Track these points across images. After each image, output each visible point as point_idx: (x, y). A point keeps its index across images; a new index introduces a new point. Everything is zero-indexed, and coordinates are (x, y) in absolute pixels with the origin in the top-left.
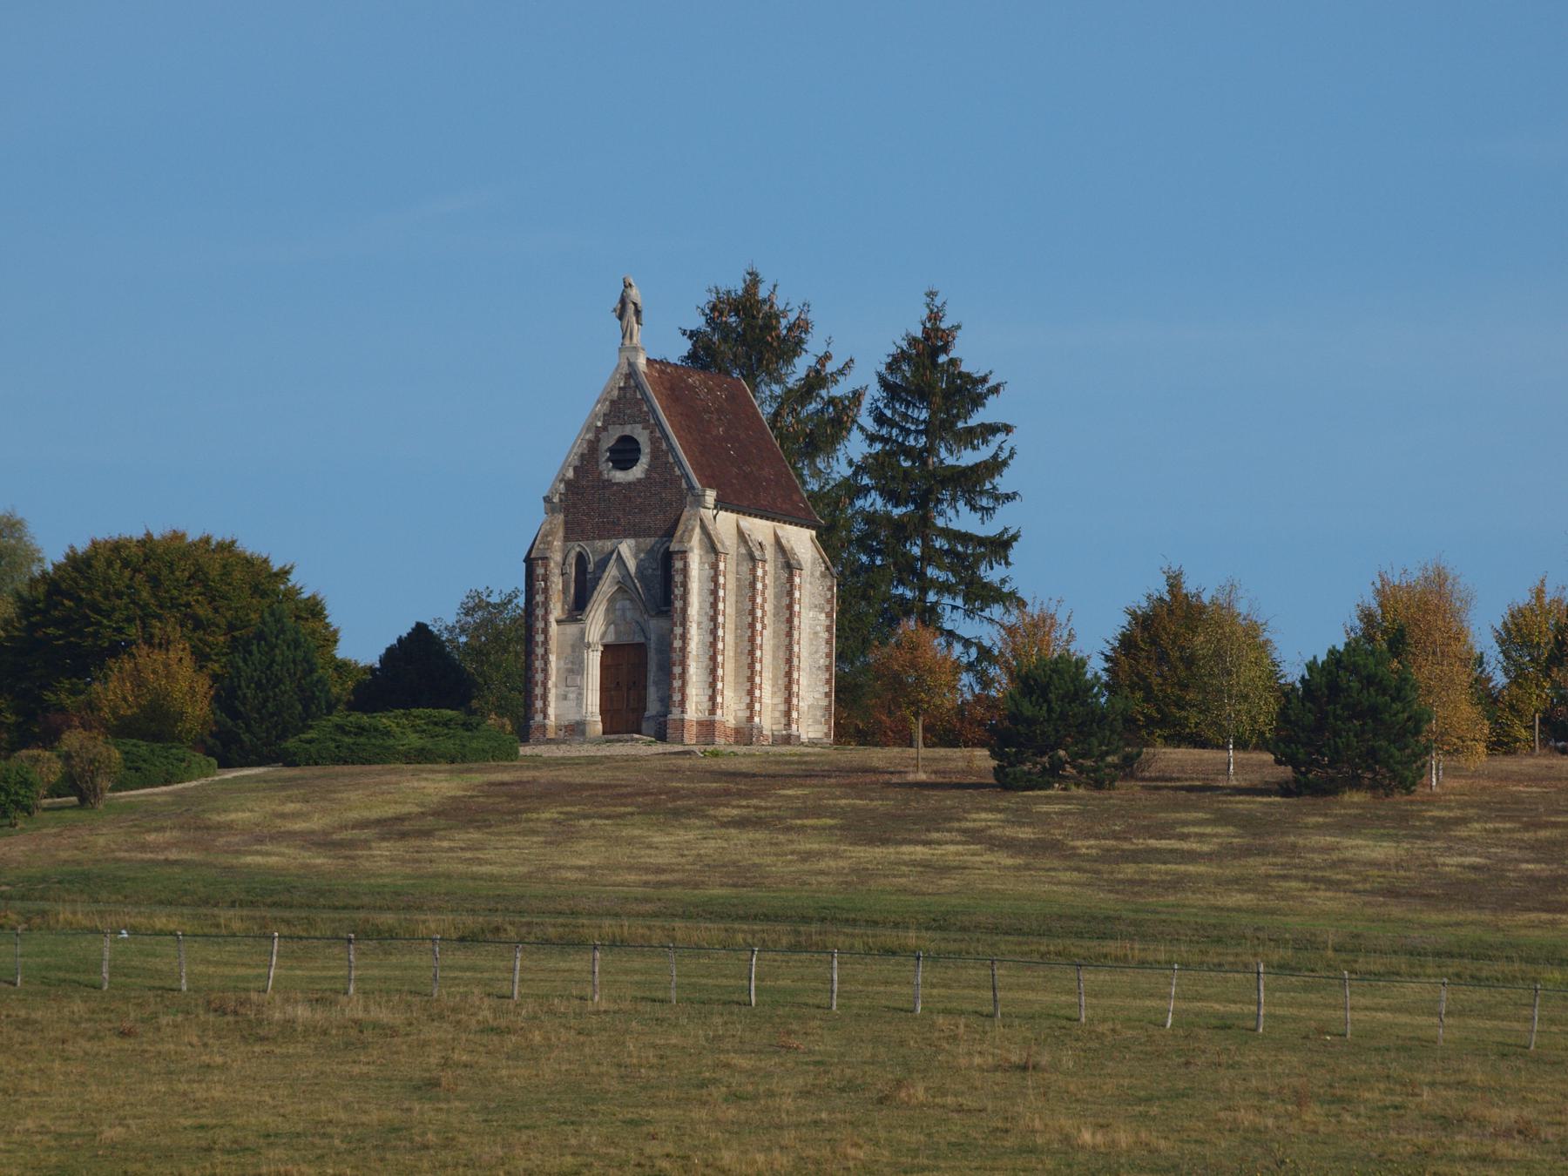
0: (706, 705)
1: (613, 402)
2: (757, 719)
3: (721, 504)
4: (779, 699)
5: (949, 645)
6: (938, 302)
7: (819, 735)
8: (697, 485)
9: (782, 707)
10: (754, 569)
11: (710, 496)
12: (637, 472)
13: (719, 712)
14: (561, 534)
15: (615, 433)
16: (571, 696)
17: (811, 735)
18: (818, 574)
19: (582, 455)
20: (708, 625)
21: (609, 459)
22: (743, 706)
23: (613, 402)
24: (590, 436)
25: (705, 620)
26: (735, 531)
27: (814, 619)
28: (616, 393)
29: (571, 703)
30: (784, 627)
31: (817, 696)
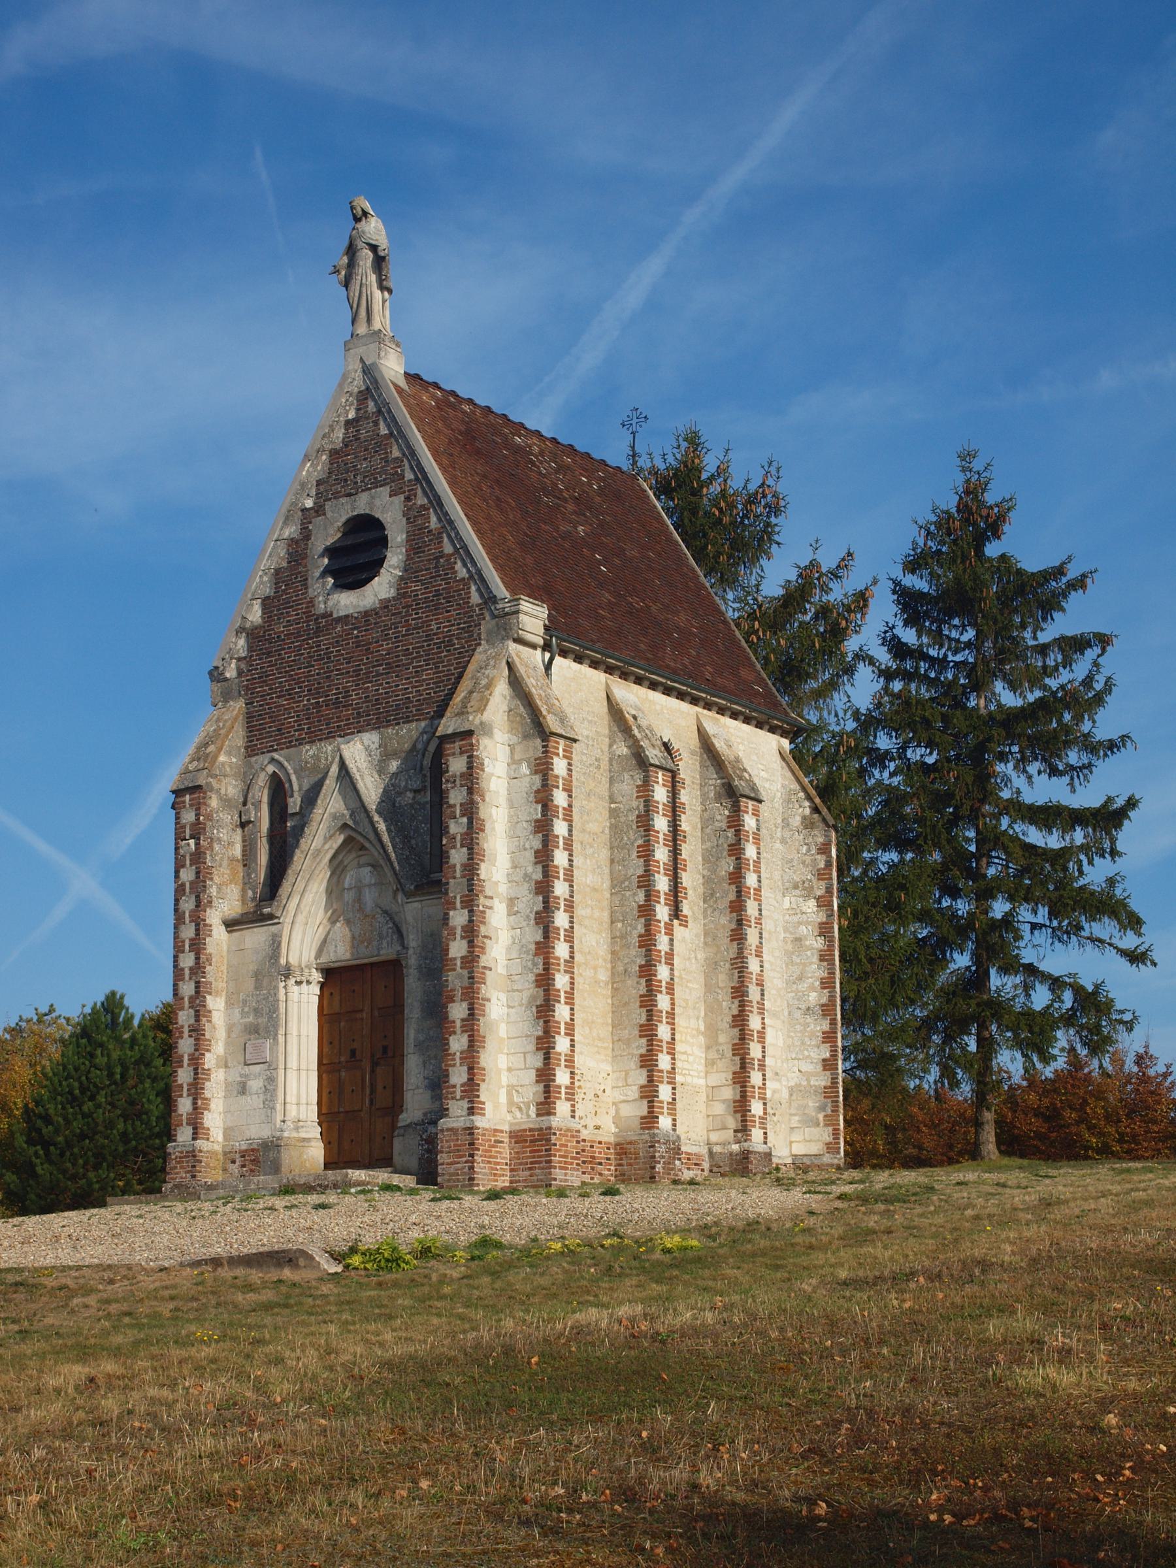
0: (531, 1092)
1: (334, 454)
2: (664, 1122)
3: (564, 639)
4: (722, 1076)
5: (1027, 988)
6: (977, 465)
7: (814, 1149)
9: (729, 1093)
10: (645, 788)
11: (533, 617)
12: (381, 588)
13: (562, 1107)
14: (238, 737)
15: (340, 513)
16: (255, 1085)
17: (799, 1149)
18: (796, 821)
19: (278, 571)
20: (530, 903)
21: (327, 572)
22: (633, 1092)
23: (334, 454)
24: (291, 531)
26: (604, 708)
27: (794, 911)
28: (339, 434)
29: (254, 1101)
30: (726, 921)
31: (807, 1067)
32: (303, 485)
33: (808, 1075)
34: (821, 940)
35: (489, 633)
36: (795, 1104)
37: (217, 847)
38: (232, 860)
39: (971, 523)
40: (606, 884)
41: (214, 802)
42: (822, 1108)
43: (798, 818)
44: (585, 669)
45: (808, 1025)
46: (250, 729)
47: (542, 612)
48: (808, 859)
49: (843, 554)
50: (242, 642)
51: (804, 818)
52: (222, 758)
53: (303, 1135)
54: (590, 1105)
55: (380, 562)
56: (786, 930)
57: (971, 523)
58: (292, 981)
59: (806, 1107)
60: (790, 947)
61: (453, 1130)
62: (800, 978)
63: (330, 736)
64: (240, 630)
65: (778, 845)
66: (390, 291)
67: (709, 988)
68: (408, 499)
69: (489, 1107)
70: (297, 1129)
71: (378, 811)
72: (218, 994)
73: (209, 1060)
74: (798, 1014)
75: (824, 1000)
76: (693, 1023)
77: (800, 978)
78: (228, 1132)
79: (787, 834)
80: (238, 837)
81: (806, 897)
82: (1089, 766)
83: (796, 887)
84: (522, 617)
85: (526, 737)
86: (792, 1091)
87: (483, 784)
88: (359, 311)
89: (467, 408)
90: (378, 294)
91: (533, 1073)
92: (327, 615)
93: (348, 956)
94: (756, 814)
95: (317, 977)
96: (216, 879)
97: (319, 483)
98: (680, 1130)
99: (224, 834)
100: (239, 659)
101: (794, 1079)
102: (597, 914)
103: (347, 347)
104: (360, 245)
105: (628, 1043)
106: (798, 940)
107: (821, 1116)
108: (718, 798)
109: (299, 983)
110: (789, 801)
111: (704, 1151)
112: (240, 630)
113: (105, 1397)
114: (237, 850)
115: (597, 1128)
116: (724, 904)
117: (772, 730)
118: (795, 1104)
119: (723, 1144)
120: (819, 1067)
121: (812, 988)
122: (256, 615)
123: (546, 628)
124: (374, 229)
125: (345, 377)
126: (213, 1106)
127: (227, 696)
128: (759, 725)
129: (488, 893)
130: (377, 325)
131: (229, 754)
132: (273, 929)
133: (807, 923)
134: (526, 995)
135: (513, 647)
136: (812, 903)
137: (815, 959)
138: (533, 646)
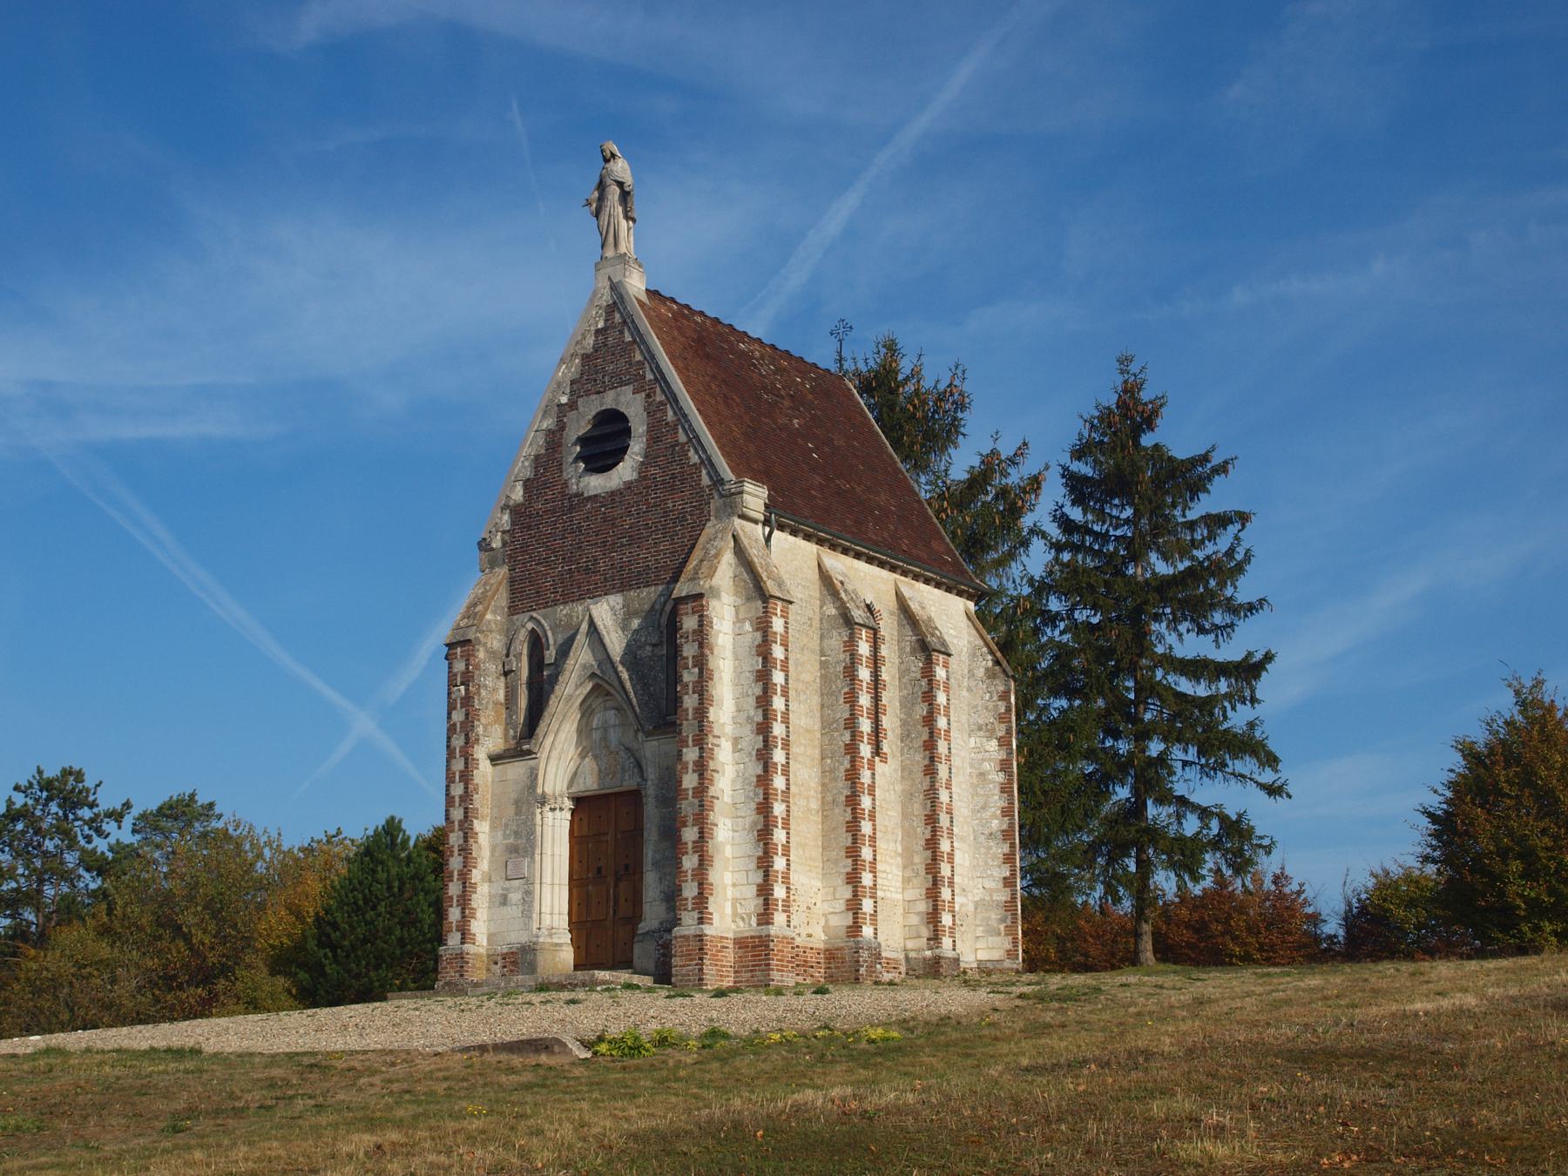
0: (753, 904)
1: (586, 358)
2: (867, 931)
3: (781, 515)
4: (917, 892)
5: (1179, 817)
6: (1134, 368)
7: (997, 955)
8: (727, 473)
9: (923, 906)
10: (851, 644)
11: (755, 497)
12: (625, 471)
13: (779, 918)
14: (502, 599)
15: (591, 408)
16: (515, 897)
17: (983, 955)
18: (981, 672)
19: (537, 457)
20: (753, 742)
21: (579, 458)
22: (840, 905)
23: (586, 358)
24: (549, 423)
25: (748, 733)
26: (814, 575)
27: (979, 750)
29: (514, 911)
30: (920, 758)
31: (990, 884)
32: (559, 385)
33: (991, 891)
34: (1001, 775)
35: (717, 510)
36: (979, 916)
37: (483, 693)
38: (496, 703)
39: (1128, 418)
40: (817, 726)
41: (481, 654)
42: (1003, 920)
43: (982, 670)
44: (799, 542)
45: (990, 848)
46: (513, 592)
47: (763, 492)
48: (991, 705)
49: (1019, 443)
50: (506, 517)
51: (987, 669)
52: (489, 616)
53: (556, 940)
54: (803, 916)
55: (624, 450)
56: (972, 766)
57: (1128, 418)
58: (547, 808)
59: (989, 919)
60: (975, 780)
61: (686, 937)
62: (983, 808)
63: (581, 598)
64: (505, 508)
65: (965, 693)
66: (634, 220)
67: (905, 815)
68: (648, 396)
69: (716, 917)
70: (551, 935)
71: (622, 662)
72: (483, 818)
73: (476, 875)
74: (982, 839)
75: (1005, 827)
76: (892, 845)
77: (983, 808)
78: (491, 937)
79: (973, 684)
80: (501, 684)
81: (989, 738)
82: (1232, 626)
83: (980, 729)
84: (745, 496)
85: (749, 599)
86: (977, 905)
87: (712, 640)
88: (607, 237)
89: (698, 319)
90: (623, 223)
91: (755, 888)
92: (579, 495)
93: (595, 786)
94: (946, 666)
95: (569, 804)
96: (483, 720)
97: (573, 382)
98: (881, 938)
99: (489, 682)
100: (504, 532)
101: (978, 894)
102: (809, 751)
103: (597, 267)
104: (609, 181)
105: (836, 862)
106: (982, 775)
107: (1002, 927)
108: (913, 652)
109: (552, 810)
110: (974, 655)
111: (902, 956)
112: (505, 508)
113: (390, 1161)
114: (501, 696)
115: (810, 936)
116: (919, 743)
117: (960, 594)
118: (979, 916)
119: (918, 950)
120: (1001, 885)
121: (994, 816)
122: (518, 494)
123: (767, 506)
124: (621, 168)
125: (595, 293)
126: (478, 915)
127: (493, 564)
128: (949, 590)
129: (716, 732)
130: (623, 249)
131: (494, 613)
132: (531, 763)
133: (990, 760)
134: (748, 821)
135: (737, 522)
136: (994, 743)
137: (997, 791)
138: (756, 522)
